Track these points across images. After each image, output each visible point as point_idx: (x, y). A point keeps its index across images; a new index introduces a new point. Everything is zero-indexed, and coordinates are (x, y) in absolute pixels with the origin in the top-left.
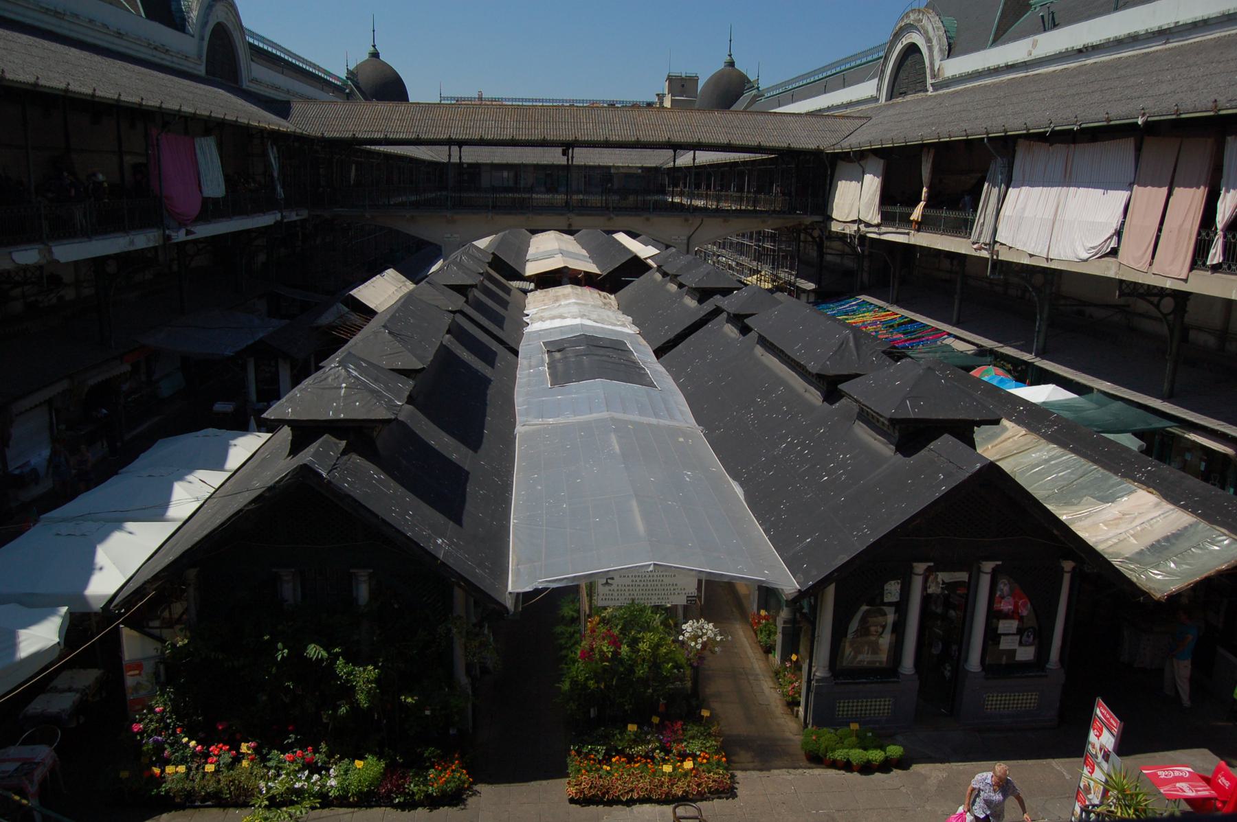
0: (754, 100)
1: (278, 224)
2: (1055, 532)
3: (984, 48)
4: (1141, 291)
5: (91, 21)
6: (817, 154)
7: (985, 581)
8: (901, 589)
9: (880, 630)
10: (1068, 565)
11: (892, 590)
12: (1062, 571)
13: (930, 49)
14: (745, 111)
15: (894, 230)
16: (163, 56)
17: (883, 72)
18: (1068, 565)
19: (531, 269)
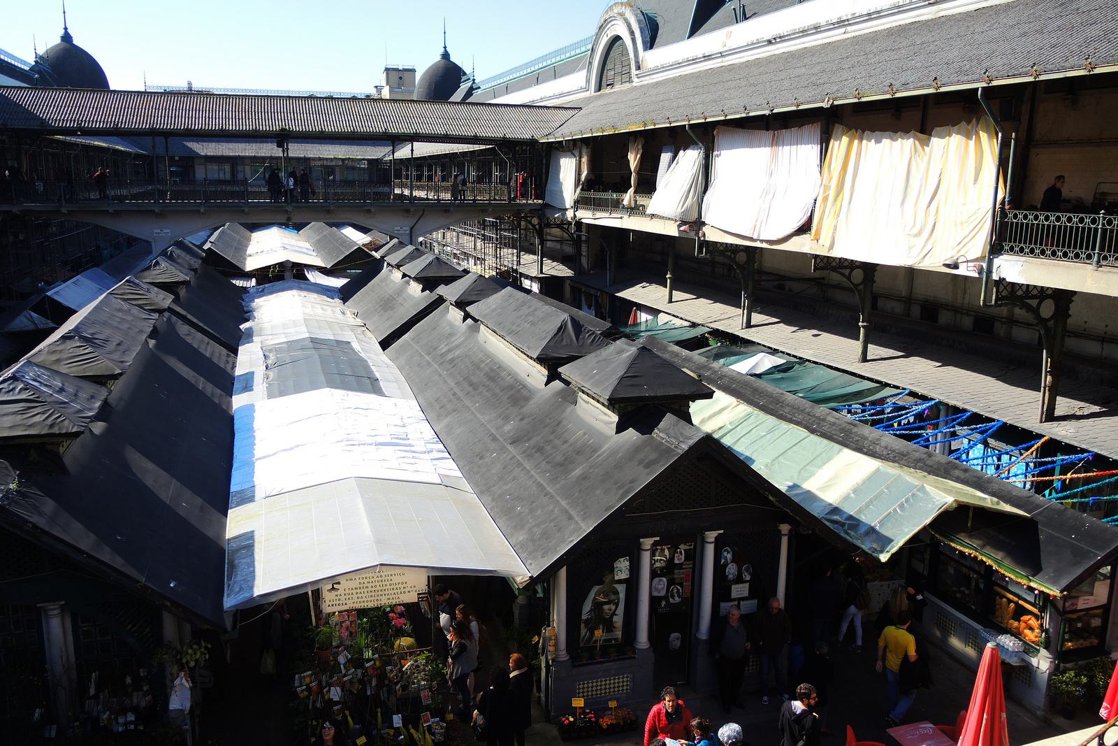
0: (470, 92)
2: (771, 498)
3: (683, 39)
4: (834, 264)
6: (533, 143)
7: (710, 550)
8: (631, 565)
9: (613, 607)
10: (785, 528)
11: (622, 568)
12: (779, 535)
13: (634, 40)
14: (463, 102)
15: (607, 215)
17: (590, 63)
18: (785, 528)
19: (251, 265)
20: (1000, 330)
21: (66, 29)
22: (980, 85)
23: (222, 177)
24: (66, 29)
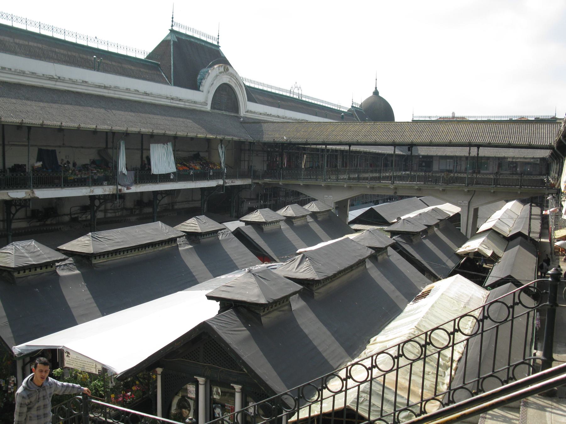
1: (218, 186)
5: (127, 89)
9: (188, 412)
11: (191, 388)
16: (178, 102)
21: (376, 88)
23: (448, 168)
24: (376, 88)
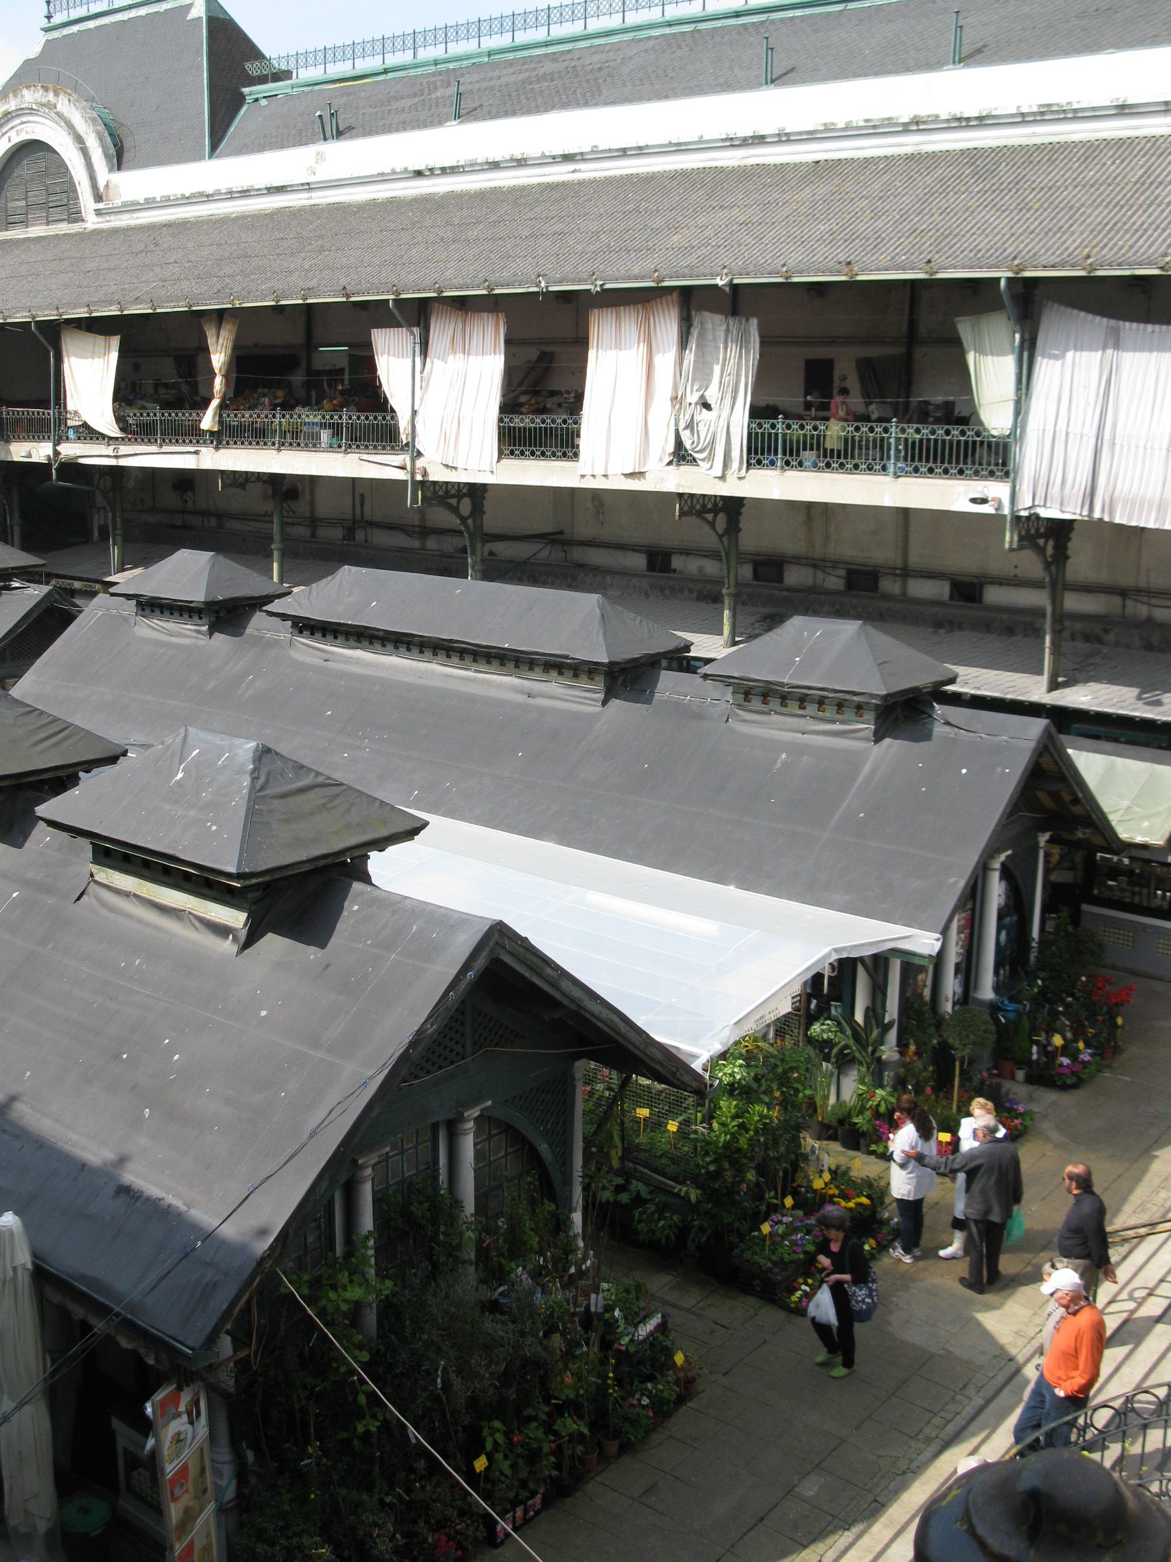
15: (154, 448)
20: (889, 585)
22: (1003, 274)
